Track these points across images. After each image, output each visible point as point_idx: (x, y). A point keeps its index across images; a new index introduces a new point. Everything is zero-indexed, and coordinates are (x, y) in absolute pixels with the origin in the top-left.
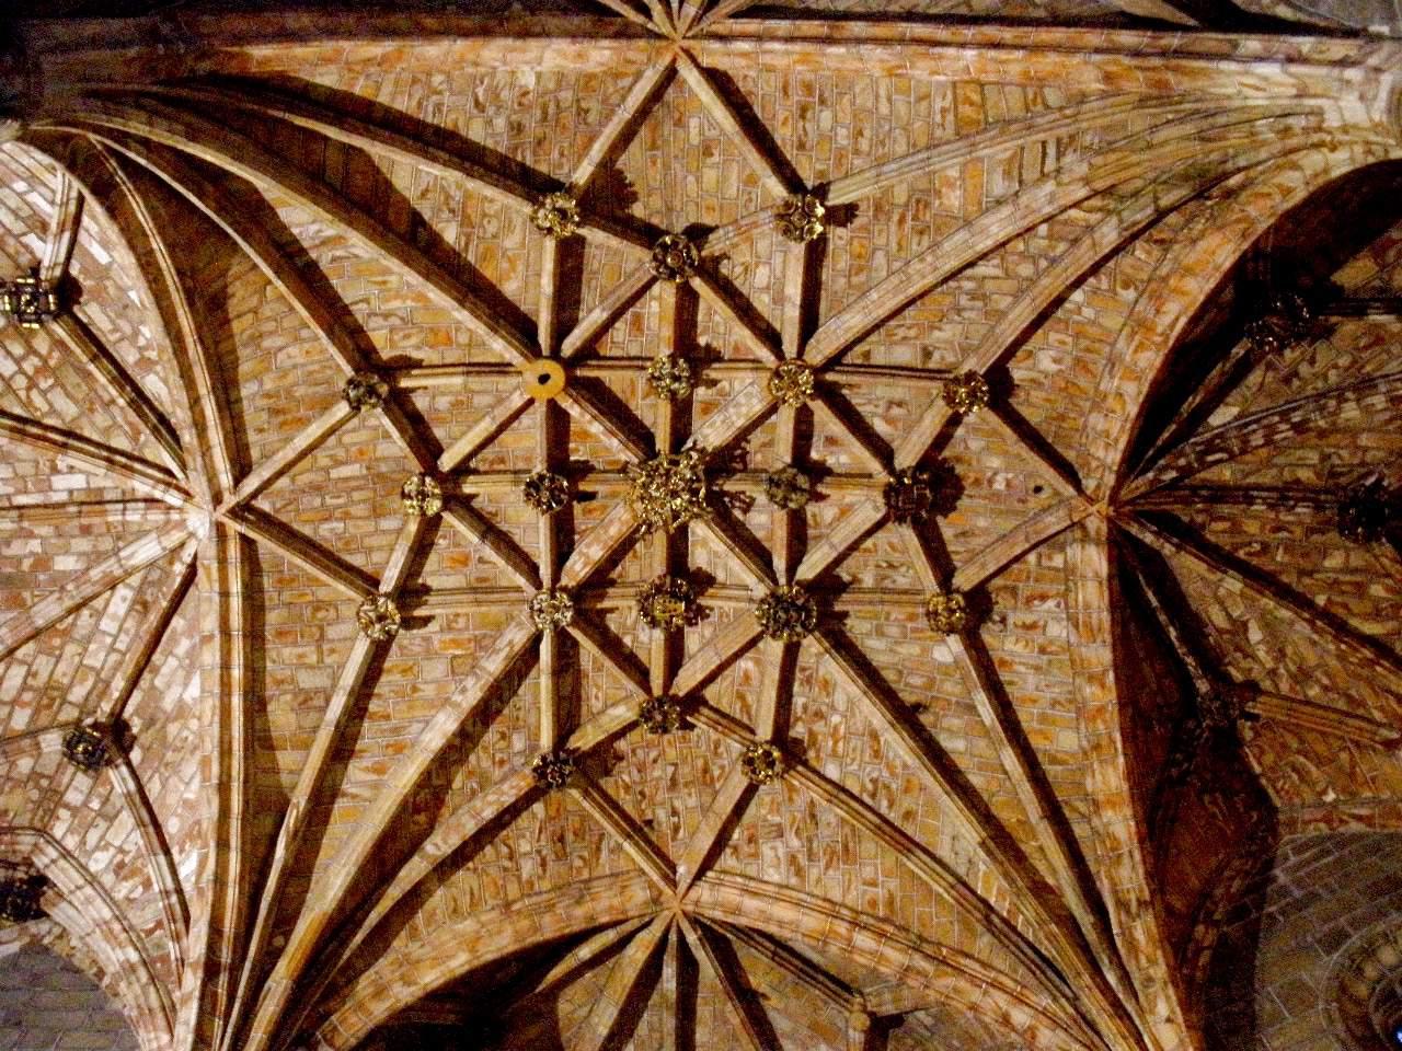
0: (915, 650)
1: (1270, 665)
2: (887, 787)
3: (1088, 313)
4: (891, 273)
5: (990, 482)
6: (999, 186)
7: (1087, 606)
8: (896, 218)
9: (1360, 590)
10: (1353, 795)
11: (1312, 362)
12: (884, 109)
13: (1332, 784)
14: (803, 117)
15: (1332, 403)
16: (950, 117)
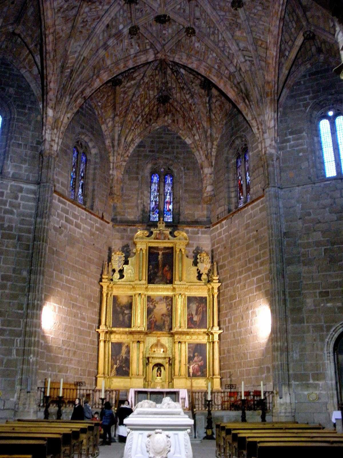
2: (86, 25)
3: (211, 56)
4: (219, 16)
5: (165, 30)
7: (140, 58)
8: (234, 19)
9: (146, 98)
10: (102, 108)
11: (196, 86)
12: (261, 23)
15: (188, 92)
16: (258, 38)
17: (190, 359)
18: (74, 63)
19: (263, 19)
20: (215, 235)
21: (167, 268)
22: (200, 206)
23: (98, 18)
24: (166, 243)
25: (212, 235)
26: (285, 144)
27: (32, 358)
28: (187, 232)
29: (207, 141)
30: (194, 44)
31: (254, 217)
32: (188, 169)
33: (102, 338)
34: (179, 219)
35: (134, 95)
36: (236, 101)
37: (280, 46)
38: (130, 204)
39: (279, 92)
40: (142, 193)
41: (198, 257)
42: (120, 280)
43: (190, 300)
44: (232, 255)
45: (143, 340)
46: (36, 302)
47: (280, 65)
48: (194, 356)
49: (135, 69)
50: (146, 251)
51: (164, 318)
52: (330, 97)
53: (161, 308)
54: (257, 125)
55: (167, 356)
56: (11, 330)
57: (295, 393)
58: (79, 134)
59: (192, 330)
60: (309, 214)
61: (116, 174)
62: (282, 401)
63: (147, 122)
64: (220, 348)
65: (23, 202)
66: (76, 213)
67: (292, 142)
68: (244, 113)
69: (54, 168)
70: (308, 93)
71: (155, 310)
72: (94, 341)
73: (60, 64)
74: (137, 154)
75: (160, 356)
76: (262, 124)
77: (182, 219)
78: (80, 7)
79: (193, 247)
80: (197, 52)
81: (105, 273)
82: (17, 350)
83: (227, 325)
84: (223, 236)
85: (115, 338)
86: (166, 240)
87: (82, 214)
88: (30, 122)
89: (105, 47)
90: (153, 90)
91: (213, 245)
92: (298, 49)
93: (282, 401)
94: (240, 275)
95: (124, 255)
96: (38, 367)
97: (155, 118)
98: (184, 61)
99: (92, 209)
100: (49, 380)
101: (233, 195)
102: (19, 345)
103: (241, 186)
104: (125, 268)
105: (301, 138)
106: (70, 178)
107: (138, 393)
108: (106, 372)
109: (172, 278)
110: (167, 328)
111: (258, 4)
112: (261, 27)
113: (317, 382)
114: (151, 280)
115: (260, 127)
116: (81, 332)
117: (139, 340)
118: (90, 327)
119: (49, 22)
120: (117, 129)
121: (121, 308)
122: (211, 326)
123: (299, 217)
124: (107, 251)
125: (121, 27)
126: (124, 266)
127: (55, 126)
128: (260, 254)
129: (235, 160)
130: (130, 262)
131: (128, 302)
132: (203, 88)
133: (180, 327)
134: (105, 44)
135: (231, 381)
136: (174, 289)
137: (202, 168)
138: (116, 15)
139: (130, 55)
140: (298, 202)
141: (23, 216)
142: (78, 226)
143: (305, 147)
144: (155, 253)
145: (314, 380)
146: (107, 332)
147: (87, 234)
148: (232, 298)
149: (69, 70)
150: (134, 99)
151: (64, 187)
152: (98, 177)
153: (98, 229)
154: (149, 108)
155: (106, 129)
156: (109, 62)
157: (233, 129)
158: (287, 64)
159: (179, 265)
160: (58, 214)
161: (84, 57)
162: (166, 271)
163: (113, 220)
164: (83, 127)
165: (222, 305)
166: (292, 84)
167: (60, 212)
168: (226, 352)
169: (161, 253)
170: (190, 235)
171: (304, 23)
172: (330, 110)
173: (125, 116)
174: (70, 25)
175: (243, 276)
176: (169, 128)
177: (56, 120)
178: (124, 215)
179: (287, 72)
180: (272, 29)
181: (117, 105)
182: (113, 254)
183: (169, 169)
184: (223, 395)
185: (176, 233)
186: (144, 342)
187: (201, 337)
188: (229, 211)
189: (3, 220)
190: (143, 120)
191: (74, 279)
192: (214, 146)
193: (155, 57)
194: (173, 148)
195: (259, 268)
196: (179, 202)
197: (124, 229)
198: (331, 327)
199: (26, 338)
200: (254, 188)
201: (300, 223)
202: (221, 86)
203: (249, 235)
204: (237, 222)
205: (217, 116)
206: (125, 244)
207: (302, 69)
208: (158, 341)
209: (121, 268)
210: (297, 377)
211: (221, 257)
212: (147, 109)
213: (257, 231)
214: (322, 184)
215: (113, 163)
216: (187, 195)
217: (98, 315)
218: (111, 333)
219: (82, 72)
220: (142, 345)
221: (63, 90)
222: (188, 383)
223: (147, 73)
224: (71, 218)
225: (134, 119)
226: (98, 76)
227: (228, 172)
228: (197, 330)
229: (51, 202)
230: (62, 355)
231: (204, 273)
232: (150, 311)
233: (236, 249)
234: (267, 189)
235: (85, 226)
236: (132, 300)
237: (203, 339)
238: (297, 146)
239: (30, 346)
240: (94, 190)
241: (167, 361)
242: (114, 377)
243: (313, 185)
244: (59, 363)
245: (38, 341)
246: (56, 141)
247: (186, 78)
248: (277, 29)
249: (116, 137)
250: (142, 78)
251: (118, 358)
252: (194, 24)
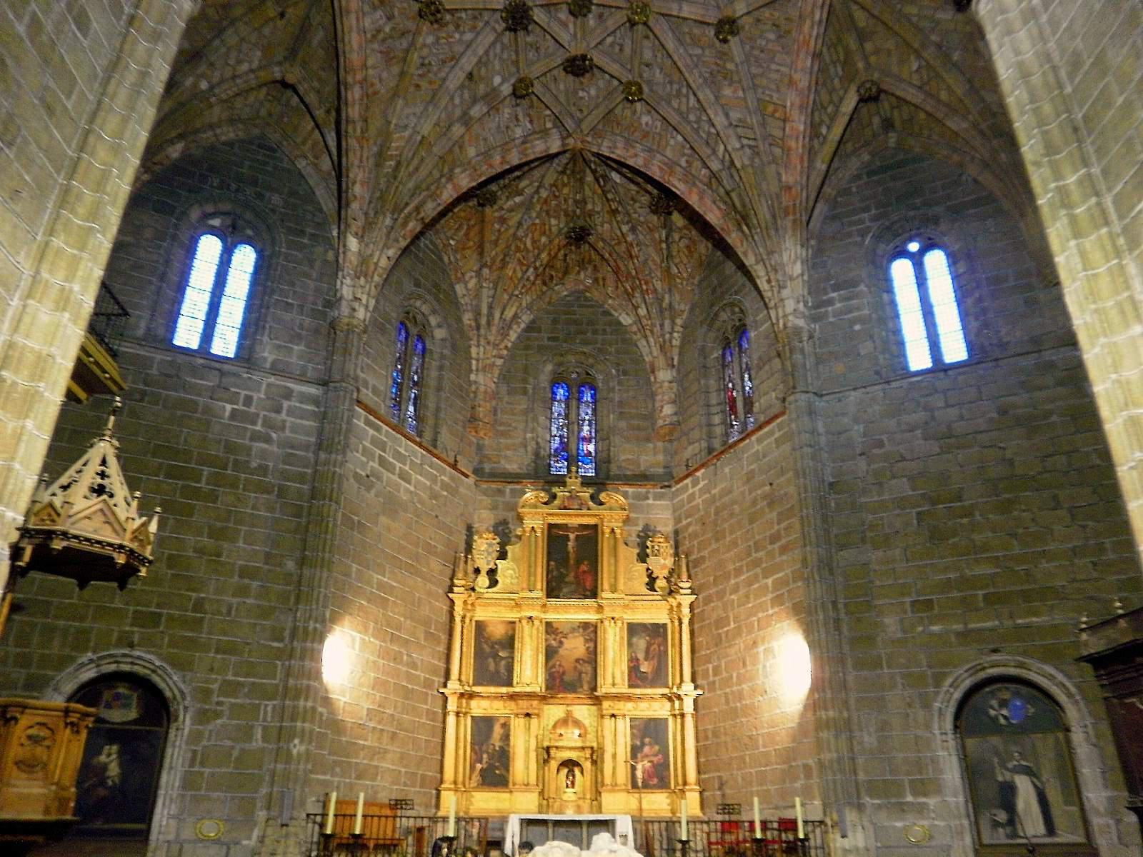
0: (497, 67)
1: (505, 207)
3: (672, 142)
4: (691, 56)
5: (583, 90)
6: (735, 115)
7: (533, 147)
8: (718, 61)
10: (456, 251)
12: (773, 67)
13: (458, 242)
14: (774, 25)
15: (626, 219)
16: (767, 99)
17: (635, 751)
18: (404, 147)
19: (778, 58)
20: (683, 500)
21: (584, 567)
22: (651, 445)
23: (453, 58)
24: (583, 516)
25: (675, 501)
26: (823, 310)
27: (297, 747)
28: (625, 495)
29: (663, 319)
30: (639, 118)
31: (764, 457)
32: (625, 373)
33: (452, 705)
34: (609, 470)
35: (520, 224)
36: (722, 229)
37: (812, 112)
38: (509, 441)
39: (811, 203)
40: (535, 419)
41: (649, 544)
42: (490, 590)
43: (633, 629)
44: (718, 537)
45: (536, 711)
46: (311, 625)
47: (811, 153)
48: (643, 744)
49: (524, 167)
50: (542, 532)
51: (579, 666)
52: (912, 213)
53: (575, 647)
54: (767, 273)
55: (588, 744)
56: (253, 683)
57: (874, 824)
58: (411, 296)
59: (638, 691)
60: (880, 444)
61: (483, 381)
62: (846, 843)
63: (544, 283)
64: (696, 727)
65: (293, 419)
66: (402, 450)
67: (838, 305)
68: (740, 251)
69: (358, 353)
70: (866, 209)
71: (561, 651)
72: (434, 713)
73: (375, 149)
74: (524, 343)
75: (573, 745)
76: (776, 271)
77: (614, 470)
78: (417, 33)
79: (637, 525)
80: (646, 135)
81: (460, 575)
82: (265, 728)
83: (711, 679)
84: (699, 501)
85: (479, 708)
86: (584, 511)
87: (414, 453)
88: (311, 263)
89: (466, 120)
90: (557, 218)
91: (678, 520)
92: (847, 118)
93: (846, 843)
94: (736, 576)
95: (498, 540)
96: (309, 766)
97: (560, 275)
98: (619, 153)
99: (435, 447)
100: (334, 796)
101: (717, 419)
102: (269, 719)
103: (733, 400)
104: (499, 566)
105: (856, 296)
106: (390, 382)
107: (527, 823)
108: (460, 779)
109: (596, 587)
110: (586, 687)
111: (768, 27)
112: (774, 76)
113: (923, 800)
114: (552, 591)
115: (772, 277)
116: (408, 694)
118: (428, 684)
119: (354, 58)
120: (486, 293)
121: (492, 647)
122: (678, 681)
123: (858, 451)
124: (464, 532)
125: (497, 80)
126: (498, 561)
127: (362, 271)
128: (779, 531)
129: (720, 352)
130: (509, 555)
131: (506, 633)
132: (654, 212)
133: (614, 685)
134: (465, 113)
135: (723, 796)
136: (600, 608)
137: (653, 372)
138: (487, 53)
139: (514, 140)
140: (856, 420)
141: (292, 447)
142: (404, 477)
143: (866, 312)
145: (915, 793)
146: (462, 695)
147: (425, 496)
148: (721, 622)
149: (393, 163)
150: (520, 233)
151: (378, 396)
152: (447, 385)
153: (445, 486)
154: (549, 254)
155: (464, 292)
156: (471, 152)
157: (714, 291)
158: (829, 149)
159: (609, 561)
160: (364, 448)
161: (423, 137)
162: (584, 572)
163: (477, 471)
164: (417, 284)
165: (699, 639)
166: (834, 193)
167: (367, 444)
168: (710, 735)
169: (572, 536)
170: (631, 501)
171: (860, 65)
172: (911, 240)
173: (504, 264)
174: (396, 69)
175: (743, 577)
176: (588, 294)
177: (364, 260)
178: (499, 462)
179: (824, 167)
180: (796, 77)
181: (487, 246)
182: (476, 537)
183: (588, 374)
184: (705, 827)
185: (603, 497)
186: (538, 715)
187: (656, 705)
188: (710, 450)
189: (249, 455)
190: (537, 276)
191: (395, 584)
192: (677, 328)
193: (563, 145)
194: (595, 332)
195: (778, 560)
196: (608, 438)
197: (499, 490)
198: (945, 675)
199: (287, 702)
200: (762, 401)
201: (862, 464)
202: (693, 200)
203: (754, 494)
204: (727, 470)
205: (682, 267)
206: (501, 518)
207: (854, 164)
208: (569, 713)
209: (492, 566)
210: (873, 789)
211: (695, 543)
212: (544, 256)
213: (771, 484)
214: (905, 383)
215: (478, 360)
216: (623, 424)
217: (444, 660)
218: (471, 696)
219: (417, 169)
220: (534, 721)
221: (380, 202)
222: (631, 801)
223: (546, 178)
224: (391, 460)
225: (519, 275)
226: (450, 179)
227: (706, 376)
228: (649, 691)
229: (349, 422)
230: (366, 740)
231: (661, 576)
232: (550, 653)
233: (726, 526)
234: (791, 398)
235: (419, 477)
236: (514, 630)
237: (661, 709)
238: (850, 312)
239: (293, 719)
240: (438, 409)
241: (588, 756)
242: (476, 789)
243: (886, 386)
244: (356, 758)
245: (314, 709)
246: (364, 301)
247: (621, 190)
248: (807, 76)
249: (485, 310)
250: (537, 192)
251: (484, 748)
252: (641, 76)
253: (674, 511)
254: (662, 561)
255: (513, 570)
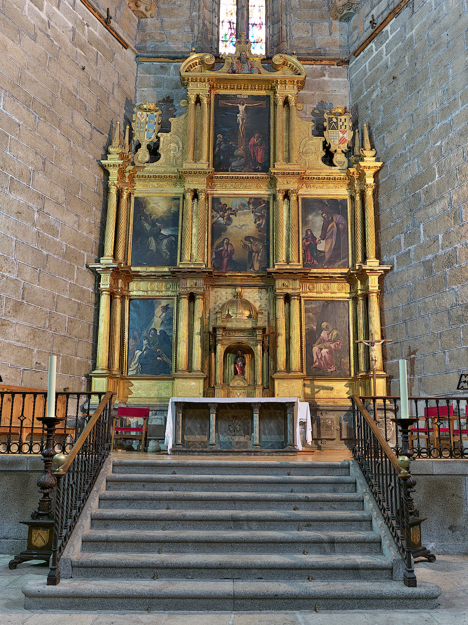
21: (254, 140)
48: (320, 330)
71: (230, 229)
72: (83, 291)
75: (243, 326)
95: (160, 112)
104: (162, 139)
117: (193, 290)
131: (169, 210)
136: (272, 181)
144: (226, 109)
162: (255, 145)
169: (241, 108)
187: (334, 286)
197: (162, 67)
206: (164, 95)
208: (238, 296)
231: (339, 150)
253: (352, 86)
254: (341, 135)
255: (177, 143)
